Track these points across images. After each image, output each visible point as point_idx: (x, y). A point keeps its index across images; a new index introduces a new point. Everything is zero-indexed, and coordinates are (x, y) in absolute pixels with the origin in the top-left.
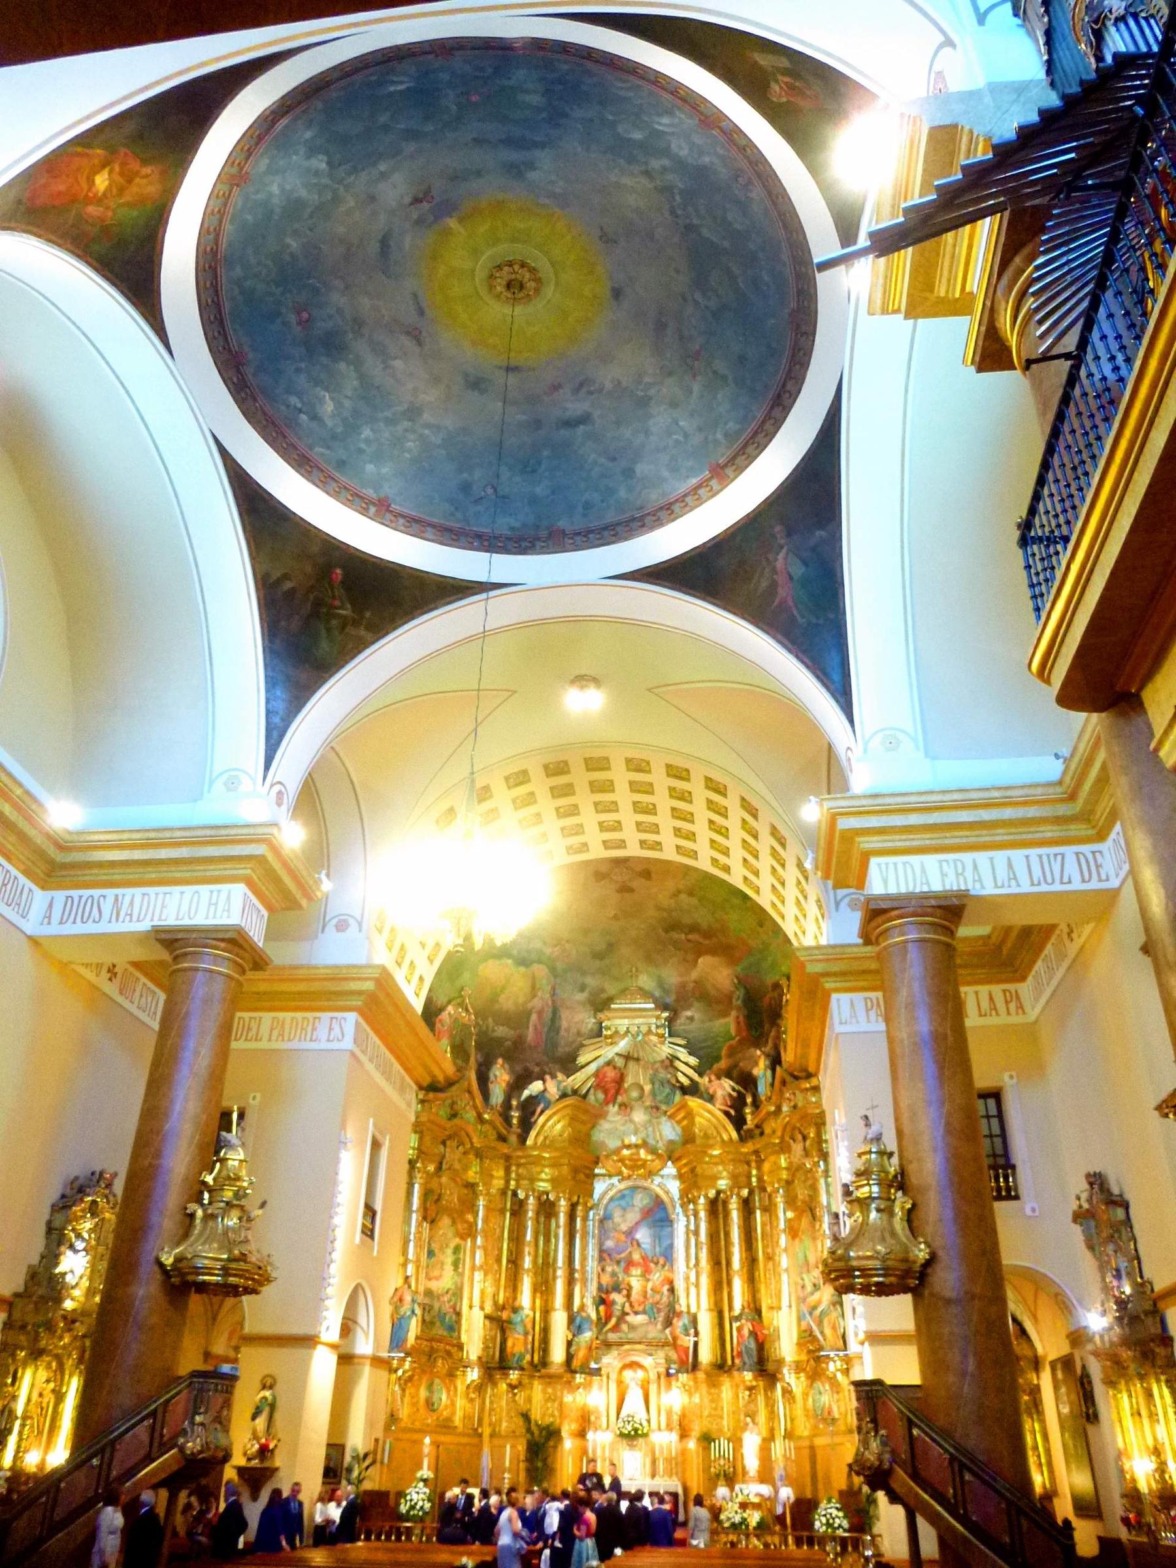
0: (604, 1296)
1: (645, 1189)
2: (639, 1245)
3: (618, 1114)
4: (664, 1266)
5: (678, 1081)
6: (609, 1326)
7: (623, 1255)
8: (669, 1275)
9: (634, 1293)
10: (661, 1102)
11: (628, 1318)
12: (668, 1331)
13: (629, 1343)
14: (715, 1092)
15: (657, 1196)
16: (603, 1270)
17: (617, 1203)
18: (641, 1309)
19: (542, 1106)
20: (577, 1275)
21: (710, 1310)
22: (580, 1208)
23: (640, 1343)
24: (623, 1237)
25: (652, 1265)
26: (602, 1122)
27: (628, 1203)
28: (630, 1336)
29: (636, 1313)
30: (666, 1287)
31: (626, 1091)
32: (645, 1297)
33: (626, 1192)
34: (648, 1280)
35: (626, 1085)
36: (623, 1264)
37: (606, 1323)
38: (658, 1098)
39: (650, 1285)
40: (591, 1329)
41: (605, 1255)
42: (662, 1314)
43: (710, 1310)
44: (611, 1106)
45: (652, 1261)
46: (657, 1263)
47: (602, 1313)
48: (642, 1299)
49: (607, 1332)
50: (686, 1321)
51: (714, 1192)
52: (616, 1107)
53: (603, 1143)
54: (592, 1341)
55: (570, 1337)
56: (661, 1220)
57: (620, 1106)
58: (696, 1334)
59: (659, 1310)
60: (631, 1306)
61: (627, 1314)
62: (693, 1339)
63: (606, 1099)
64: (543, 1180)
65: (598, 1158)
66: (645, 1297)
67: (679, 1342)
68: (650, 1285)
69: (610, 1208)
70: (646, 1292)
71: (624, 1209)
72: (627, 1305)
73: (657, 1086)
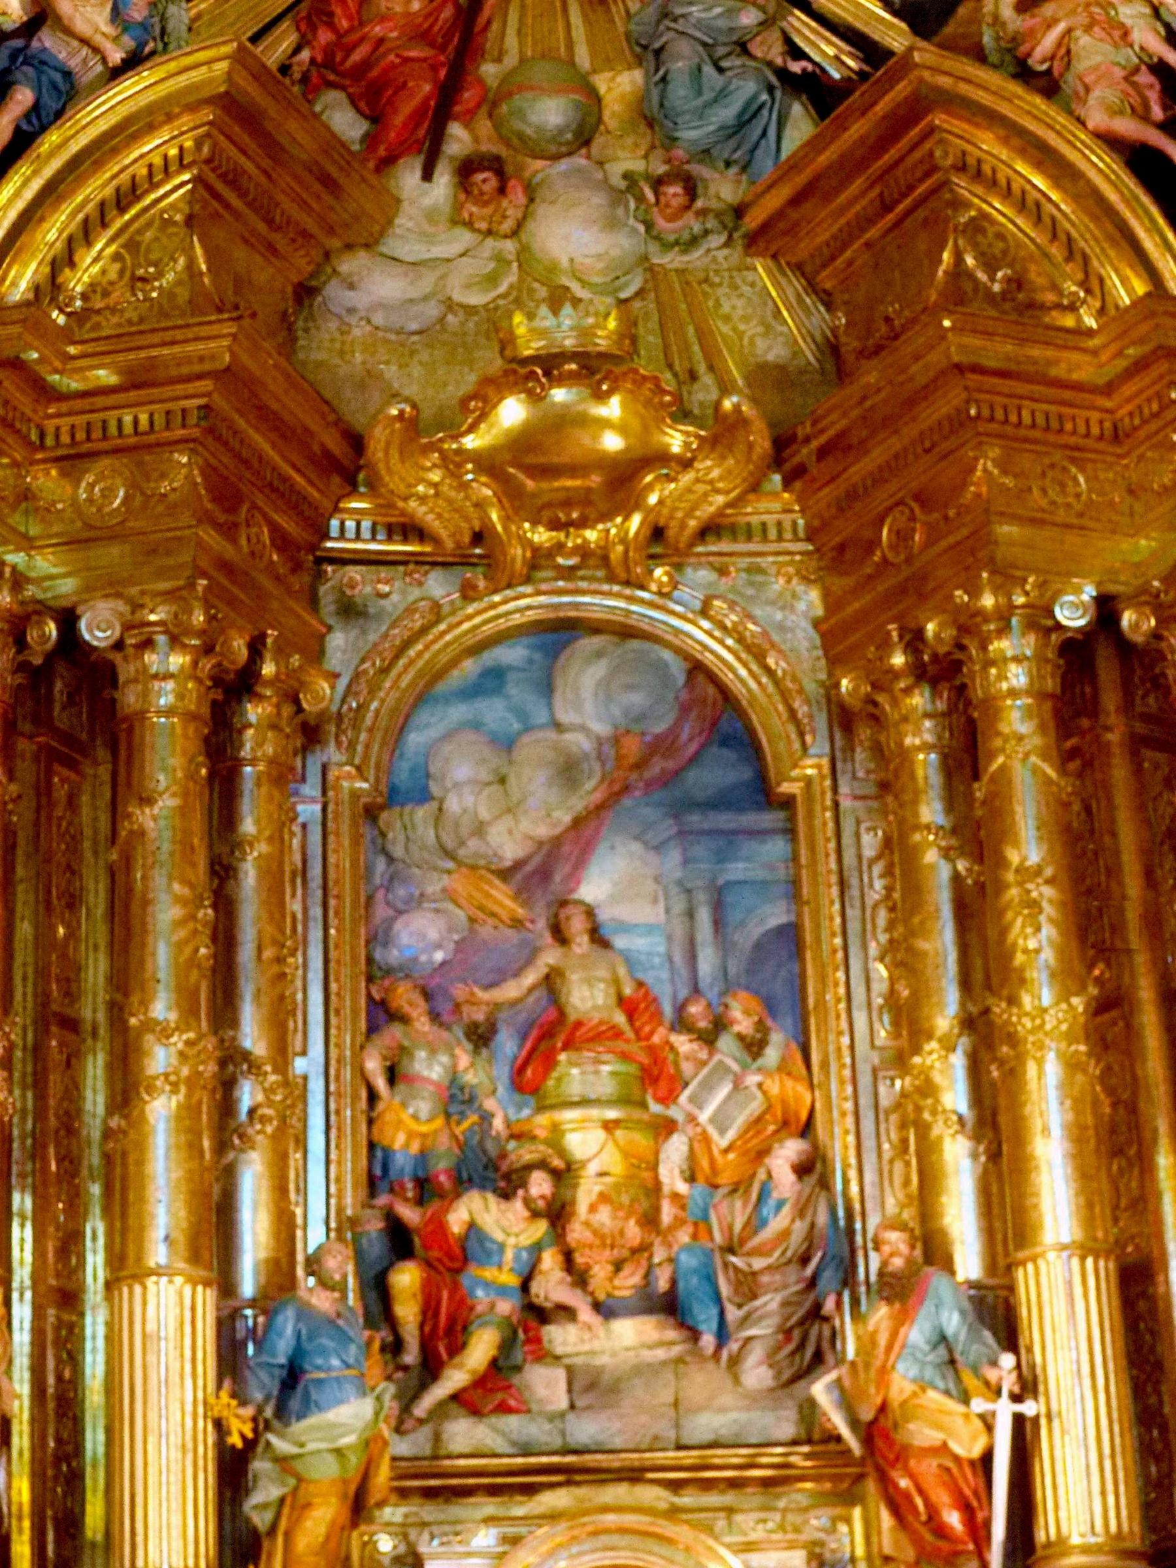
0: (409, 1214)
1: (626, 632)
2: (598, 938)
3: (457, 220)
4: (754, 1047)
5: (796, 53)
6: (455, 1379)
7: (511, 990)
8: (800, 1096)
9: (586, 1193)
10: (705, 154)
11: (559, 1337)
12: (820, 1389)
13: (570, 1475)
14: (1065, 52)
15: (697, 669)
16: (393, 1075)
17: (458, 712)
18: (628, 1282)
19: (23, 97)
20: (247, 1095)
21: (1085, 1249)
22: (254, 712)
23: (634, 1475)
24: (502, 897)
25: (683, 1043)
26: (348, 265)
27: (522, 714)
28: (585, 1430)
29: (605, 1310)
30: (790, 1150)
31: (492, 102)
32: (650, 1221)
33: (512, 654)
34: (667, 1127)
35: (489, 71)
36: (507, 1044)
37: (431, 1369)
38: (691, 134)
39: (675, 1150)
40: (363, 1391)
41: (405, 997)
42: (770, 1303)
43: (1085, 1249)
44: (408, 177)
45: (681, 1023)
46: (709, 1038)
47: (407, 1312)
48: (634, 1232)
49: (440, 1412)
50: (953, 1322)
51: (1089, 592)
52: (444, 179)
53: (369, 379)
54: (371, 1444)
55: (239, 1430)
56: (720, 802)
57: (466, 169)
58: (1028, 1387)
59: (748, 1287)
60: (578, 1277)
61: (567, 1312)
62: (1005, 1411)
63: (370, 141)
64: (27, 543)
65: (357, 442)
66: (650, 1221)
67: (921, 1434)
68: (675, 1150)
69: (415, 739)
70: (656, 1189)
71: (506, 745)
72: (550, 1260)
73: (679, 66)
